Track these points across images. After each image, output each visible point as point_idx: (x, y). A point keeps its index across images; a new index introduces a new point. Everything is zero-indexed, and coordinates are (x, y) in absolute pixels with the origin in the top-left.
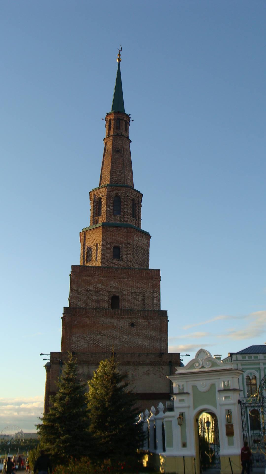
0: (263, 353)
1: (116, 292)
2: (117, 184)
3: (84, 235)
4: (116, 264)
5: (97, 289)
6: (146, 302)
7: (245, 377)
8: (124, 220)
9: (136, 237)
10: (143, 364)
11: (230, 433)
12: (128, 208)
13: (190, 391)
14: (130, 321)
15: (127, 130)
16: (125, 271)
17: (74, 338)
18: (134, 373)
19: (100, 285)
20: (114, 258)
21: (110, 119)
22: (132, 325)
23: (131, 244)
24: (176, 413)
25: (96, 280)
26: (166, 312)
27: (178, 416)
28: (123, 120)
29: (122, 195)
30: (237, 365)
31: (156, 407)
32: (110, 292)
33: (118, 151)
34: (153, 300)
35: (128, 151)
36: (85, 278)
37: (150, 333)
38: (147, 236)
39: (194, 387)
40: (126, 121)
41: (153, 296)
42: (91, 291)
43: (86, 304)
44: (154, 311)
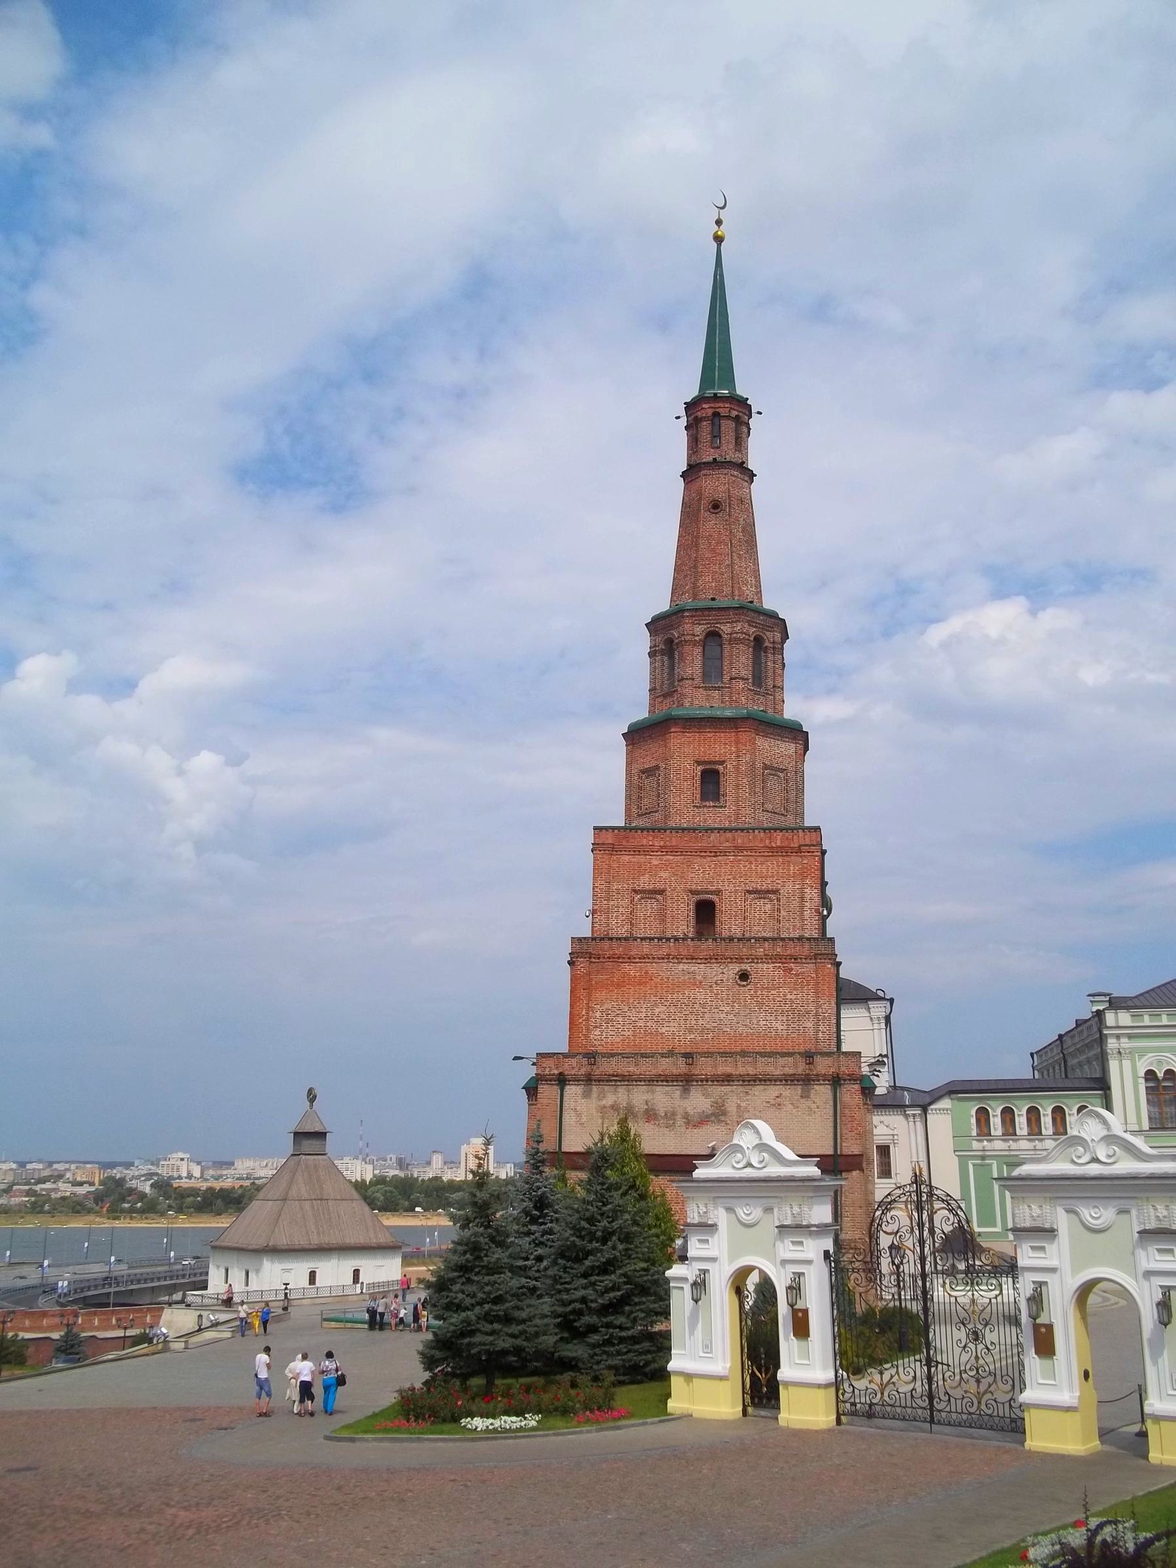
1: (707, 893)
2: (713, 599)
4: (711, 817)
5: (659, 886)
6: (783, 913)
8: (731, 697)
9: (762, 743)
11: (801, 1327)
12: (740, 662)
15: (740, 442)
16: (729, 835)
17: (598, 1014)
18: (743, 1104)
19: (664, 875)
20: (703, 798)
21: (696, 419)
22: (744, 976)
23: (747, 763)
25: (656, 863)
27: (691, 1279)
28: (728, 417)
29: (726, 629)
32: (691, 891)
33: (716, 506)
34: (802, 907)
35: (746, 503)
36: (627, 858)
37: (789, 996)
38: (797, 734)
40: (737, 419)
41: (802, 898)
43: (632, 924)
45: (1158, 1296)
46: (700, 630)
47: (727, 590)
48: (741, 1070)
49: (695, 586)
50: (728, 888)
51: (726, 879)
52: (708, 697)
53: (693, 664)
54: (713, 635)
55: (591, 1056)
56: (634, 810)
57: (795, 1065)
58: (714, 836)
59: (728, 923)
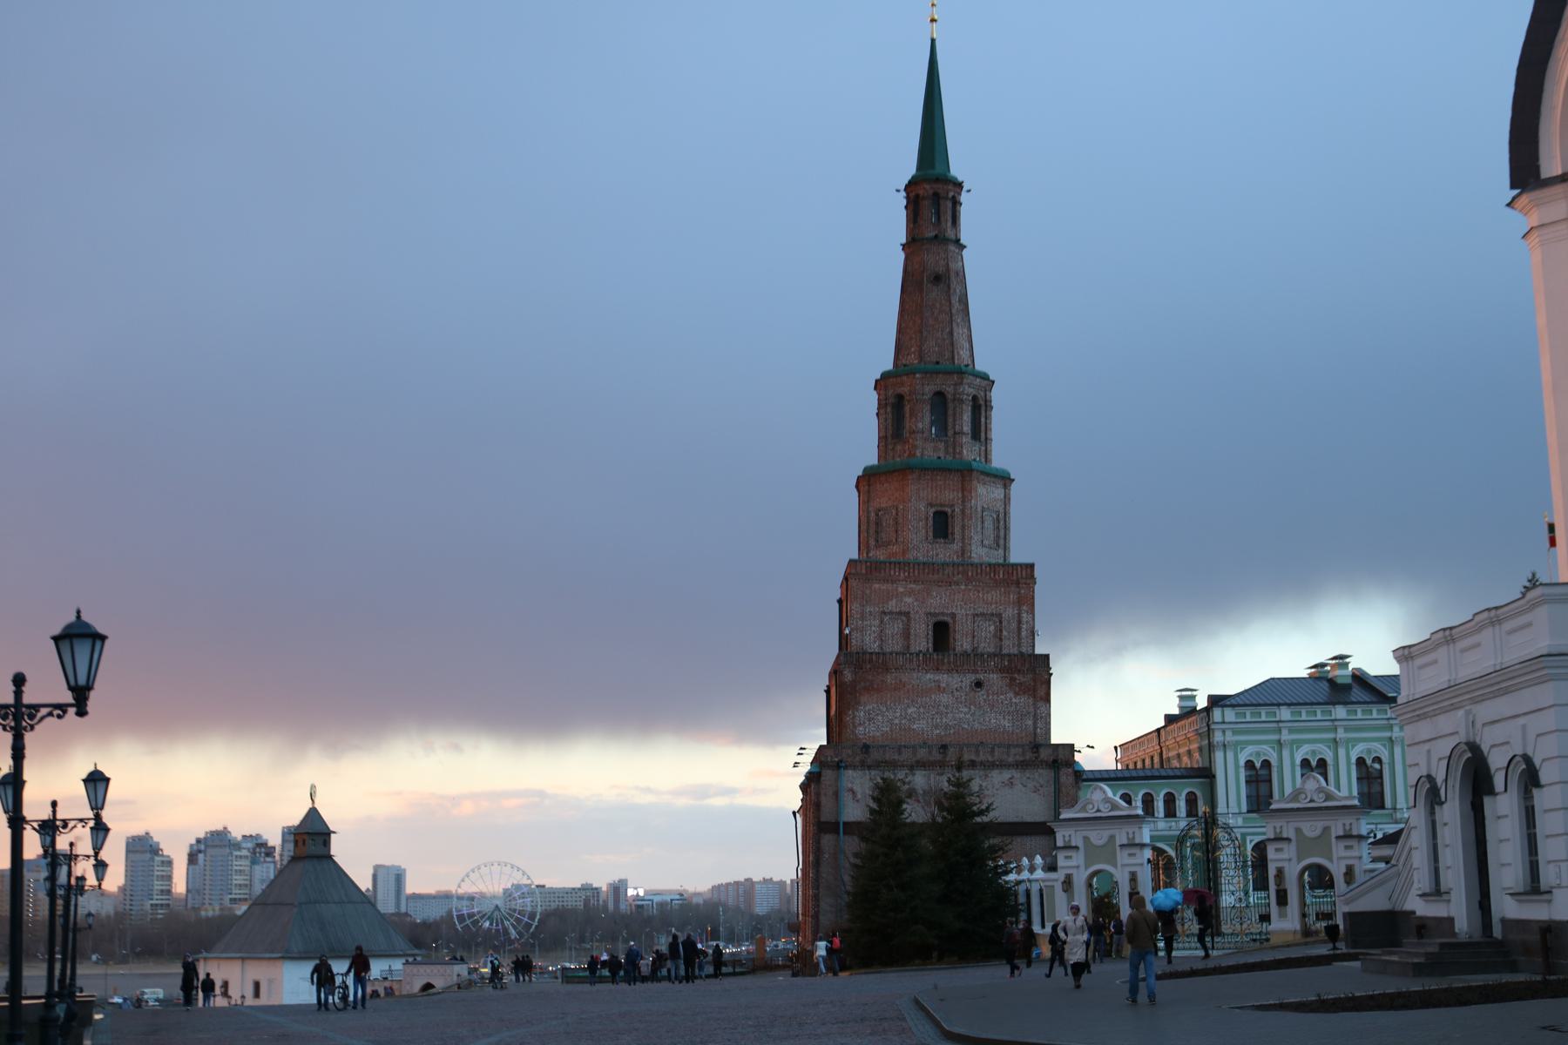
0: (1289, 705)
3: (868, 481)
4: (944, 553)
7: (1242, 762)
10: (1002, 765)
13: (1080, 844)
14: (971, 678)
19: (909, 600)
20: (935, 537)
21: (917, 196)
22: (979, 684)
24: (1060, 876)
26: (1047, 656)
27: (1062, 878)
29: (949, 390)
30: (1224, 732)
31: (1031, 858)
33: (937, 279)
34: (1019, 629)
38: (1005, 480)
39: (1086, 839)
41: (1020, 622)
42: (891, 613)
44: (1022, 654)
45: (1344, 870)
46: (927, 389)
47: (948, 355)
48: (982, 757)
49: (920, 351)
50: (960, 612)
51: (956, 603)
52: (936, 449)
53: (923, 421)
54: (940, 394)
55: (866, 748)
56: (872, 542)
57: (1024, 754)
58: (949, 570)
59: (962, 643)
